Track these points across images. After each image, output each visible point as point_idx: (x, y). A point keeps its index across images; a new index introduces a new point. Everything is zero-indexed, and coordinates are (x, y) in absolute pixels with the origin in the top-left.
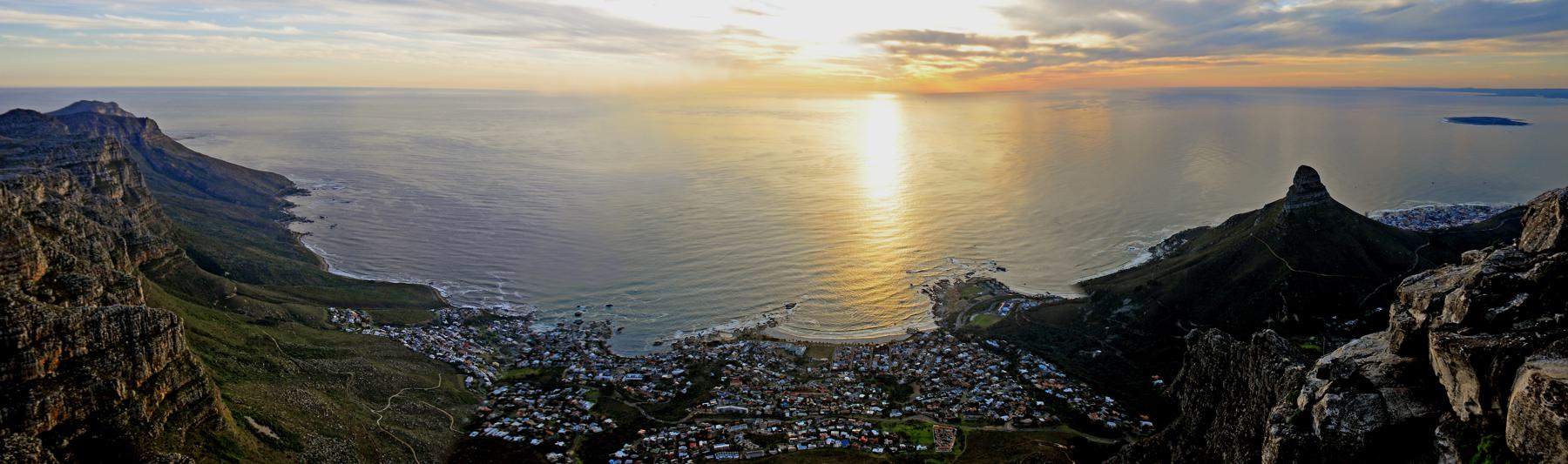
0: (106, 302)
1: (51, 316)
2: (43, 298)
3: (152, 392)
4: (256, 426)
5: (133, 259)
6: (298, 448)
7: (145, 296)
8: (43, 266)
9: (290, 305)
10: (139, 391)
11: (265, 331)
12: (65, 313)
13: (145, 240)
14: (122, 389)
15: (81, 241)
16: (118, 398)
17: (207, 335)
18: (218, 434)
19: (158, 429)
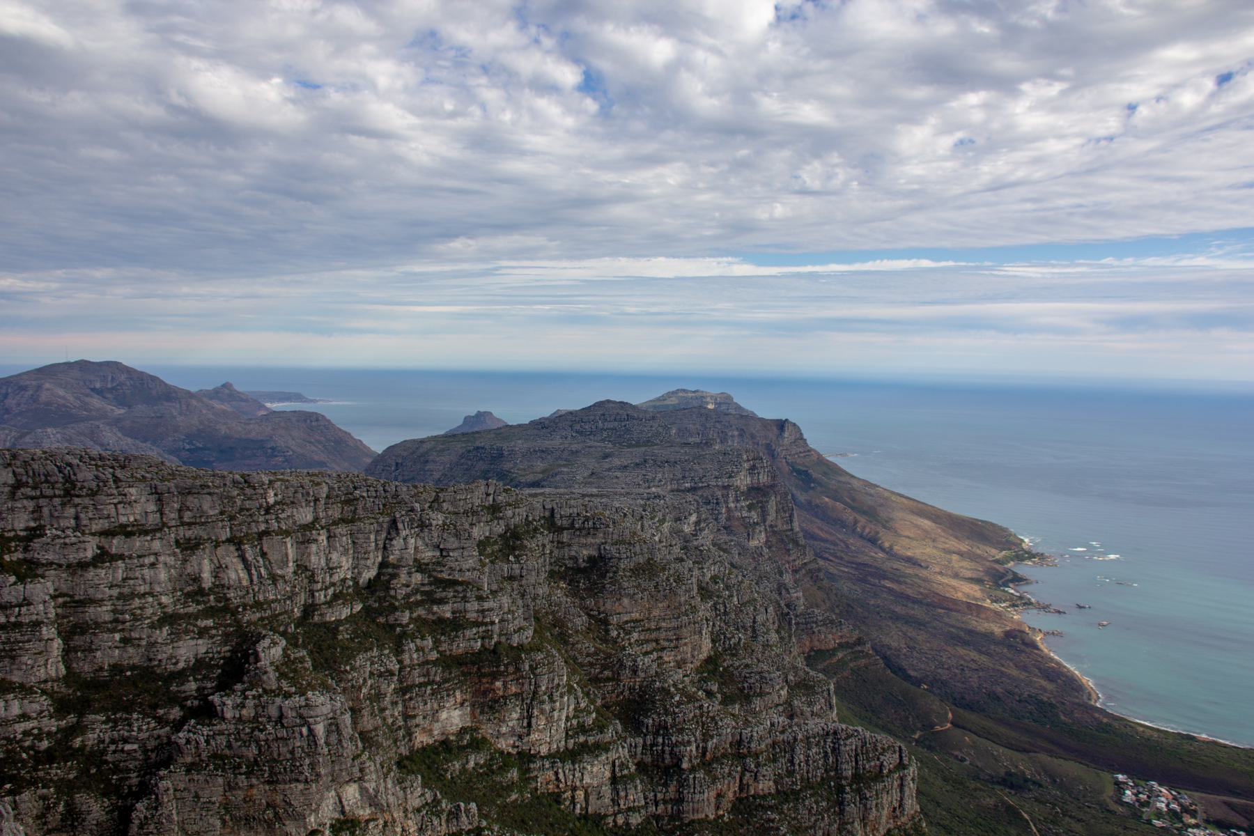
1: (728, 727)
8: (706, 647)
15: (739, 611)
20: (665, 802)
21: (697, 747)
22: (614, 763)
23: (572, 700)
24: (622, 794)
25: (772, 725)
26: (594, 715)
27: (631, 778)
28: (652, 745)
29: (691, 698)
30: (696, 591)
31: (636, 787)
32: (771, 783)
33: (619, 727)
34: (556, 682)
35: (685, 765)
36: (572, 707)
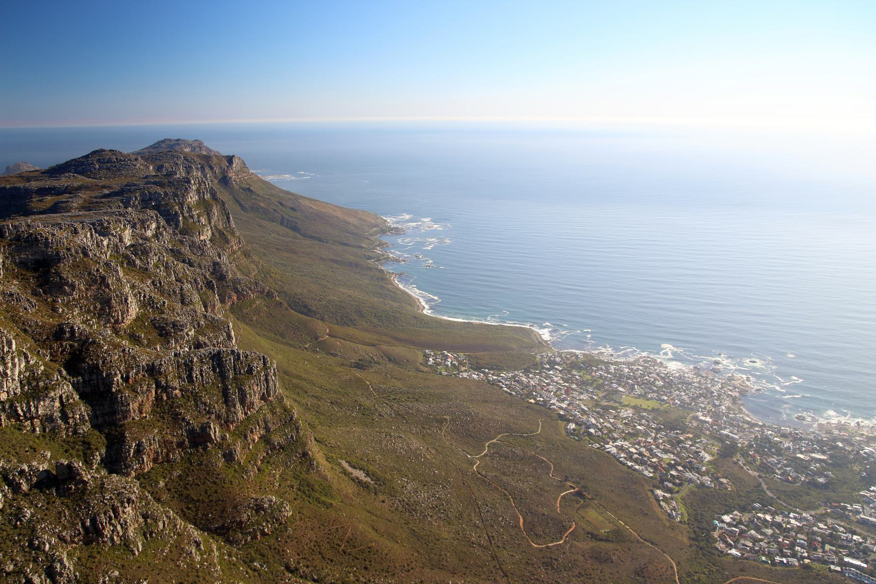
0: (198, 346)
1: (144, 360)
2: (134, 339)
3: (246, 437)
4: (350, 469)
5: (222, 301)
6: (392, 493)
7: (239, 338)
8: (134, 310)
9: (384, 347)
10: (233, 434)
11: (359, 374)
12: (158, 356)
13: (236, 282)
14: (215, 431)
15: (171, 283)
16: (210, 440)
17: (298, 377)
18: (312, 477)
19: (253, 472)
20: (103, 415)
21: (122, 377)
22: (61, 397)
23: (23, 358)
24: (71, 415)
25: (176, 355)
26: (42, 368)
27: (76, 404)
28: (89, 381)
29: (116, 346)
30: (121, 274)
31: (80, 409)
32: (177, 391)
33: (64, 373)
34: (6, 349)
35: (114, 390)
36: (23, 365)
